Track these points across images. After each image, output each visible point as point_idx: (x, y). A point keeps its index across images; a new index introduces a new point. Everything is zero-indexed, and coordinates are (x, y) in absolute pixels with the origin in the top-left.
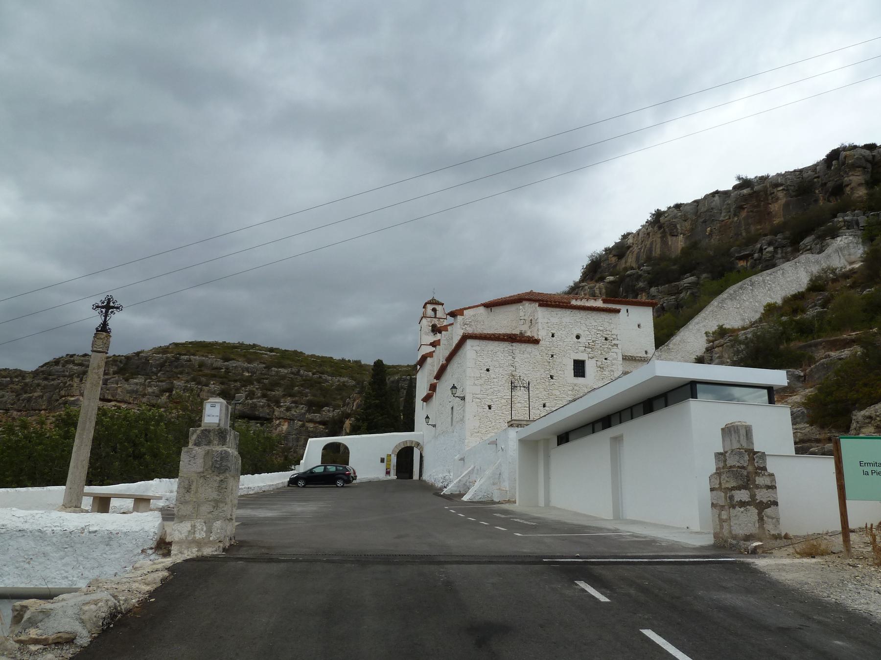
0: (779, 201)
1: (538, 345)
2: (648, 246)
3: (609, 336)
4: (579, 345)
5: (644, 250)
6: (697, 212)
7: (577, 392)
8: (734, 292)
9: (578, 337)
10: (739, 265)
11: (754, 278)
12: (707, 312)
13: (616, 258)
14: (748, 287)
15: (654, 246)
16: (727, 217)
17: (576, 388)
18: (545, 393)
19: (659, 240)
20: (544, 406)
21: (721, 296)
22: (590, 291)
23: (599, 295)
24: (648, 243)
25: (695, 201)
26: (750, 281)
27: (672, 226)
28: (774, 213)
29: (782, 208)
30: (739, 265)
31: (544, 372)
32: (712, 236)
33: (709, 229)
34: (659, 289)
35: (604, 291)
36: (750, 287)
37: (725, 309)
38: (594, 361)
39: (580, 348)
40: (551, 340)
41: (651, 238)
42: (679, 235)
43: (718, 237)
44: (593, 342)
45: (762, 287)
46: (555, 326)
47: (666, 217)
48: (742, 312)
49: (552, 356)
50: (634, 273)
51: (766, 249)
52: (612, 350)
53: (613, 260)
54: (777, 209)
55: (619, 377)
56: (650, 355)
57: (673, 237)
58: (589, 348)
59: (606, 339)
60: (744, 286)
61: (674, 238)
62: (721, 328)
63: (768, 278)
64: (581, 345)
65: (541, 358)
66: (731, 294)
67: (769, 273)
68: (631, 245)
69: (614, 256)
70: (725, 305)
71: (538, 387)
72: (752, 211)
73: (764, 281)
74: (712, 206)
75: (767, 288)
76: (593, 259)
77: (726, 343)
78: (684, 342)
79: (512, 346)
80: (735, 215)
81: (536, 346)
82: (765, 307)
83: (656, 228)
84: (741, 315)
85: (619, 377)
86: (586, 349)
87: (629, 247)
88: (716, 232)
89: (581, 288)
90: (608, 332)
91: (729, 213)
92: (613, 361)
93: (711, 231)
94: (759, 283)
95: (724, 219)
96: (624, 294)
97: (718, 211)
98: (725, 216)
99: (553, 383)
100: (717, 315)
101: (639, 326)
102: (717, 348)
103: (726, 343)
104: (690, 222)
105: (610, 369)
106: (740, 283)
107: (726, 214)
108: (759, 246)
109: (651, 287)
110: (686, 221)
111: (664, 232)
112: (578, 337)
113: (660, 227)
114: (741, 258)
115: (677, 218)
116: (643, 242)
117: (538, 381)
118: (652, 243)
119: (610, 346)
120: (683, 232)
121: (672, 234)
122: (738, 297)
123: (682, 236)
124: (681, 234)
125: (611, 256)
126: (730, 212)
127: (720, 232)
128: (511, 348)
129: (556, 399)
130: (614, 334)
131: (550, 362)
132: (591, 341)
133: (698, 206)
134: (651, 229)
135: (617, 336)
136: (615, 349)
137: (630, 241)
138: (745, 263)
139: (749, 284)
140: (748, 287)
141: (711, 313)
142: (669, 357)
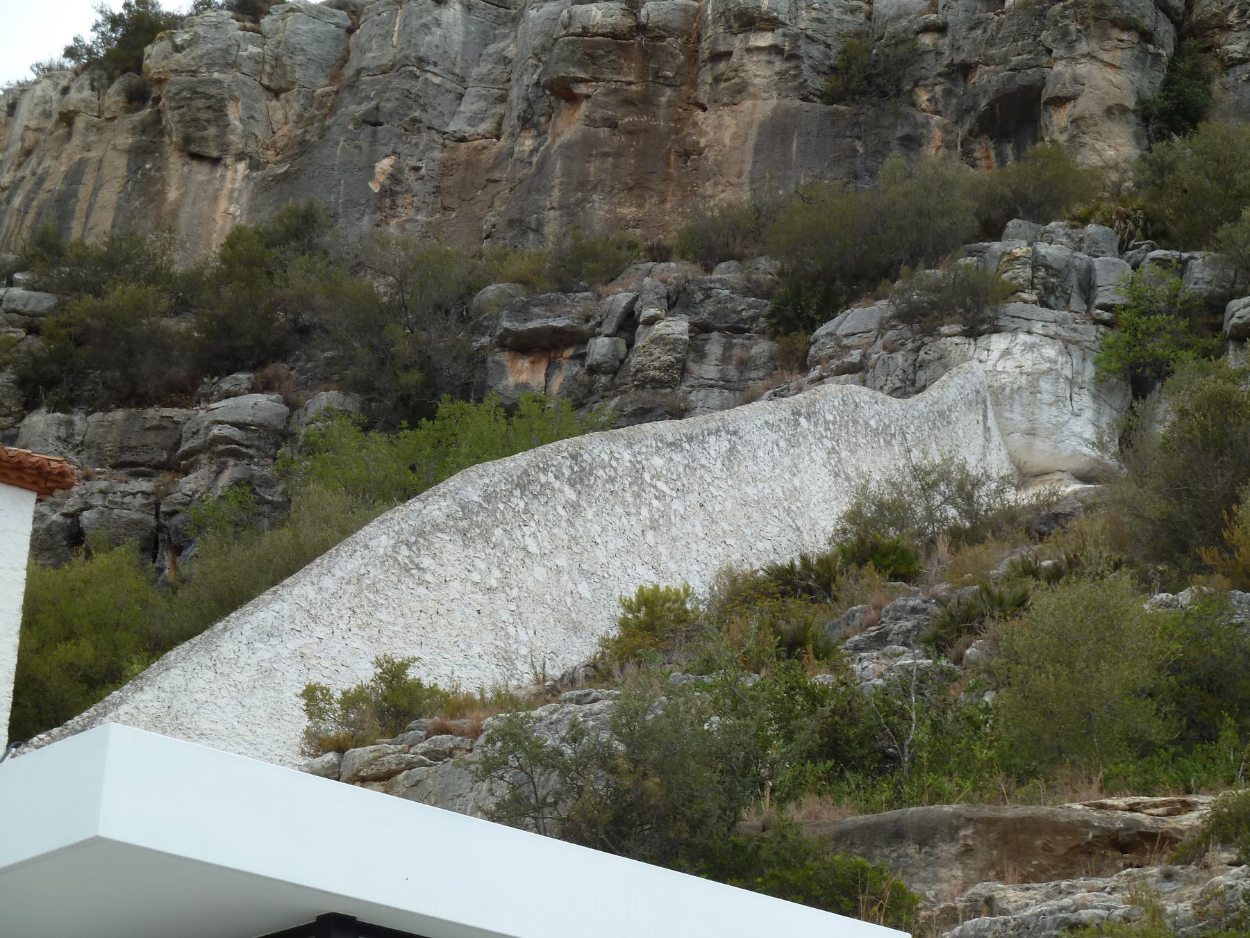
0: (747, 104)
2: (55, 183)
5: (28, 200)
6: (344, 60)
8: (487, 498)
10: (511, 380)
11: (596, 446)
12: (327, 582)
14: (557, 485)
15: (84, 192)
16: (484, 127)
19: (118, 165)
21: (414, 504)
26: (574, 457)
27: (200, 103)
28: (711, 155)
29: (751, 143)
30: (511, 380)
32: (393, 206)
33: (385, 164)
34: (70, 424)
36: (567, 488)
37: (427, 585)
41: (76, 140)
42: (229, 160)
43: (421, 217)
45: (624, 503)
47: (178, 49)
48: (505, 616)
51: (651, 321)
54: (727, 141)
57: (195, 165)
60: (543, 478)
61: (201, 172)
62: (393, 674)
63: (658, 461)
70: (426, 562)
72: (612, 124)
73: (637, 471)
74: (422, 51)
75: (644, 511)
77: (410, 766)
80: (526, 122)
82: (629, 608)
83: (114, 97)
84: (499, 629)
88: (417, 186)
91: (500, 109)
93: (395, 177)
94: (612, 480)
95: (468, 130)
97: (449, 85)
98: (474, 120)
103: (410, 766)
104: (296, 107)
106: (521, 460)
107: (482, 104)
108: (620, 299)
109: (30, 405)
110: (276, 93)
111: (155, 126)
113: (137, 97)
114: (524, 345)
115: (234, 65)
116: (28, 153)
118: (75, 175)
120: (252, 148)
121: (195, 148)
122: (498, 532)
123: (242, 167)
124: (240, 157)
126: (502, 99)
127: (437, 191)
133: (350, 31)
134: (87, 93)
138: (542, 378)
139: (567, 472)
140: (557, 485)
141: (351, 589)
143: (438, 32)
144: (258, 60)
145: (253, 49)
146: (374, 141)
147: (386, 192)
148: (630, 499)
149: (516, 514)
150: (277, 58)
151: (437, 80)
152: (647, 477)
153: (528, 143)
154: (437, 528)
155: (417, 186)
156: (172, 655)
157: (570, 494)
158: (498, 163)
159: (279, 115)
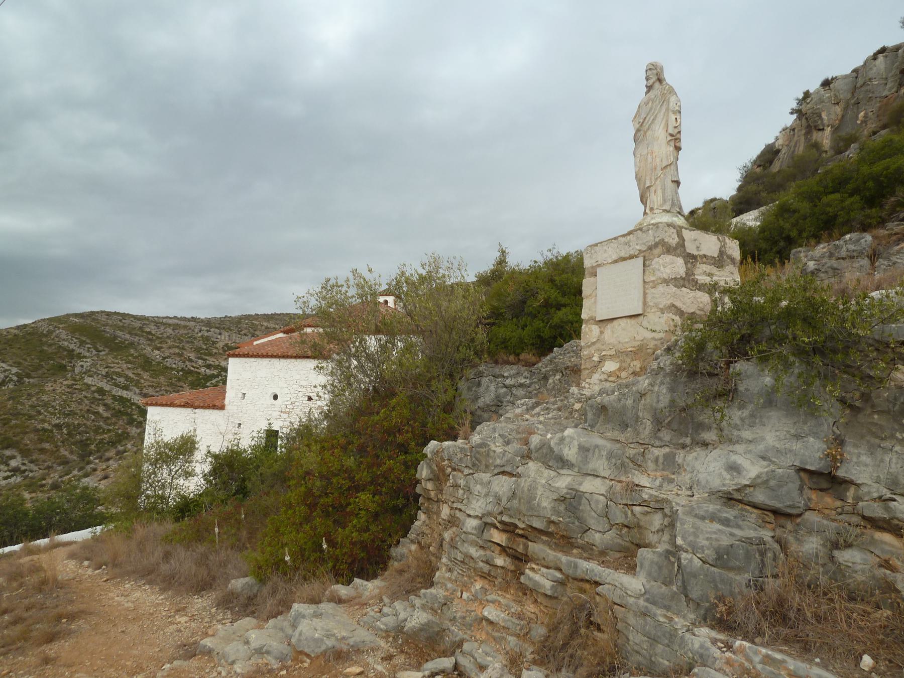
2: (792, 149)
9: (275, 397)
19: (803, 138)
25: (854, 71)
27: (815, 116)
33: (862, 114)
42: (825, 128)
46: (246, 383)
47: (808, 104)
58: (285, 412)
61: (820, 133)
64: (276, 409)
68: (780, 148)
74: (870, 76)
79: (195, 413)
86: (282, 414)
87: (778, 151)
88: (872, 117)
93: (866, 116)
97: (881, 82)
98: (890, 90)
112: (275, 397)
115: (823, 102)
120: (831, 122)
124: (828, 126)
127: (878, 116)
128: (193, 416)
143: (875, 68)
145: (827, 95)
146: (858, 108)
147: (862, 122)
151: (876, 83)
159: (839, 110)
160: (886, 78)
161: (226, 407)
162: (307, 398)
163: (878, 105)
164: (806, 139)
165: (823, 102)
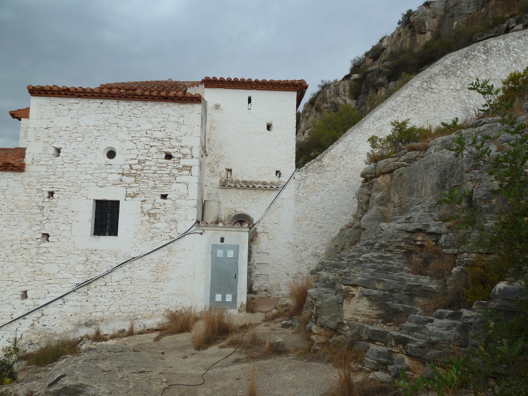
1: (22, 174)
3: (175, 150)
4: (107, 171)
7: (95, 266)
8: (454, 63)
9: (111, 154)
11: (492, 42)
12: (399, 99)
13: (372, 59)
14: (479, 55)
16: (474, 11)
17: (93, 258)
18: (29, 270)
19: (409, 39)
20: (25, 295)
22: (334, 89)
23: (343, 93)
24: (399, 43)
26: (484, 46)
27: (420, 24)
31: (30, 228)
33: (455, 23)
34: (396, 83)
35: (348, 88)
36: (483, 55)
37: (435, 93)
38: (137, 201)
39: (110, 175)
40: (51, 162)
41: (402, 38)
42: (427, 32)
44: (139, 162)
45: (504, 57)
46: (61, 133)
47: (415, 16)
48: (464, 97)
49: (51, 194)
50: (375, 68)
51: (513, 27)
52: (179, 179)
53: (369, 61)
55: (186, 234)
56: (284, 179)
57: (421, 35)
58: (129, 175)
59: (169, 156)
60: (473, 54)
61: (422, 36)
62: (400, 127)
63: (514, 43)
64: (113, 171)
65: (27, 198)
66: (446, 67)
67: (517, 36)
68: (385, 47)
69: (370, 58)
70: (434, 86)
71: (12, 258)
73: (507, 47)
75: (511, 58)
76: (355, 63)
77: (399, 167)
78: (352, 153)
80: (482, 6)
81: (18, 176)
82: (504, 83)
83: (407, 28)
84: (462, 102)
85: (186, 234)
86: (124, 178)
87: (383, 49)
89: (327, 87)
90: (174, 143)
91: (477, 6)
92: (178, 201)
93: (458, 25)
94: (499, 51)
95: (472, 12)
96: (365, 91)
97: (466, 5)
99: (45, 250)
100: (417, 103)
101: (269, 127)
102: (381, 177)
103: (399, 167)
105: (170, 216)
106: (465, 49)
107: (474, 6)
109: (390, 82)
110: (434, 18)
111: (414, 31)
112: (111, 154)
113: (411, 27)
115: (426, 15)
116: (395, 42)
117: (15, 247)
119: (175, 171)
120: (431, 28)
121: (421, 32)
122: (459, 72)
123: (429, 32)
124: (429, 31)
125: (368, 58)
127: (466, 25)
129: (50, 281)
130: (187, 147)
131: (43, 207)
132: (137, 161)
134: (402, 29)
135: (191, 149)
136: (185, 177)
137: (385, 44)
139: (482, 50)
140: (479, 55)
141: (407, 99)
142: (320, 181)
144: (430, 13)
145: (428, 11)
146: (453, 19)
148: (505, 55)
149: (465, 66)
150: (433, 11)
151: (464, 5)
152: (511, 48)
153: (484, 10)
154: (436, 75)
155: (462, 25)
156: (348, 131)
157: (484, 57)
158: (478, 16)
160: (469, 3)
161: (27, 168)
162: (164, 156)
163: (466, 18)
164: (411, 39)
165: (426, 15)
